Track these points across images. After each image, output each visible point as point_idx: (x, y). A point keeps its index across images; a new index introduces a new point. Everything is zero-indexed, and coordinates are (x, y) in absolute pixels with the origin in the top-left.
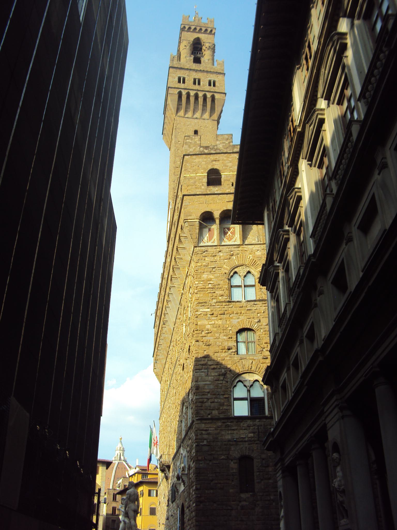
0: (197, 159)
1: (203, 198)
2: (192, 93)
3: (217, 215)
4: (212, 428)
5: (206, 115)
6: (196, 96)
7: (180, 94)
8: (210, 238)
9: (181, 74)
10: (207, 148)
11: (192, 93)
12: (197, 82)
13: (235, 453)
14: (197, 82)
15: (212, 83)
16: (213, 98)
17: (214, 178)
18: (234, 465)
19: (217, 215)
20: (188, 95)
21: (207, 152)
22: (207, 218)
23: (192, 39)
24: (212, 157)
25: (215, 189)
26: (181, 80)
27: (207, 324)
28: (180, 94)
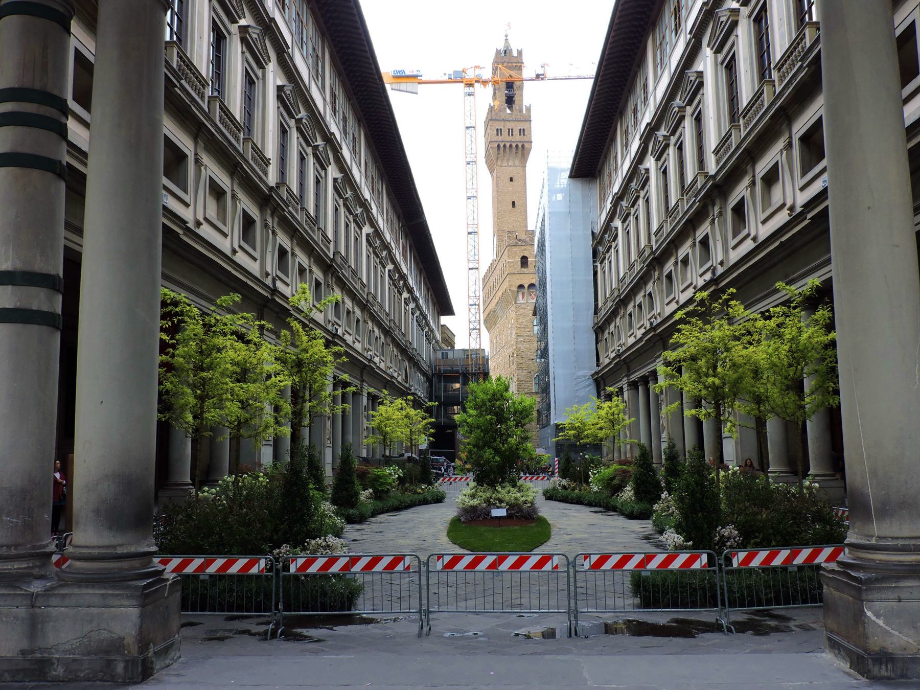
0: (515, 249)
1: (518, 276)
2: (508, 145)
3: (526, 286)
8: (523, 297)
9: (499, 125)
10: (520, 240)
11: (508, 145)
14: (511, 132)
15: (522, 132)
16: (523, 146)
19: (526, 286)
20: (505, 146)
22: (521, 287)
24: (523, 248)
25: (525, 270)
26: (499, 132)
27: (522, 347)
28: (499, 146)
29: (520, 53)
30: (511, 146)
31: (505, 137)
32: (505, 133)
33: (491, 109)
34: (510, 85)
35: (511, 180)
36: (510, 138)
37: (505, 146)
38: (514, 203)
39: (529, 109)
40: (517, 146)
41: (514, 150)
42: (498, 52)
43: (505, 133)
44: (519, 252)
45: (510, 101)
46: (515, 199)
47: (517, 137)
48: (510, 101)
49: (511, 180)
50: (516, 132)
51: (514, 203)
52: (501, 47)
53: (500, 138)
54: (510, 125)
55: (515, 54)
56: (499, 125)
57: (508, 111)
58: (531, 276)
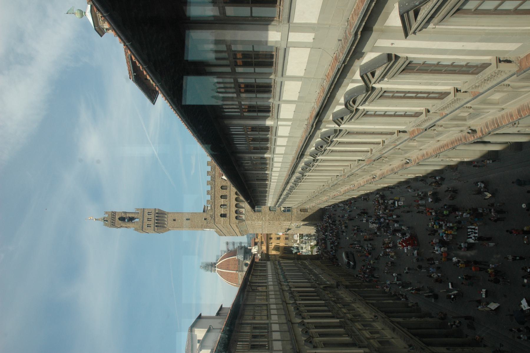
0: (216, 220)
3: (236, 215)
4: (293, 217)
5: (166, 216)
6: (157, 220)
7: (156, 226)
12: (149, 220)
13: (299, 212)
14: (149, 220)
15: (149, 213)
16: (157, 213)
17: (223, 216)
18: (302, 213)
19: (236, 215)
20: (156, 223)
21: (213, 217)
22: (236, 218)
23: (120, 222)
25: (228, 215)
26: (149, 226)
28: (156, 226)
29: (106, 213)
30: (157, 220)
31: (152, 223)
32: (150, 223)
33: (136, 229)
34: (122, 219)
35: (174, 220)
36: (153, 220)
37: (156, 223)
38: (187, 219)
39: (138, 209)
40: (157, 216)
41: (159, 218)
42: (106, 225)
43: (150, 223)
44: (218, 218)
45: (131, 219)
46: (185, 219)
47: (152, 216)
48: (131, 219)
49: (174, 220)
50: (150, 217)
51: (187, 219)
52: (102, 223)
53: (152, 226)
54: (146, 220)
55: (107, 216)
56: (145, 226)
57: (136, 220)
58: (231, 212)
